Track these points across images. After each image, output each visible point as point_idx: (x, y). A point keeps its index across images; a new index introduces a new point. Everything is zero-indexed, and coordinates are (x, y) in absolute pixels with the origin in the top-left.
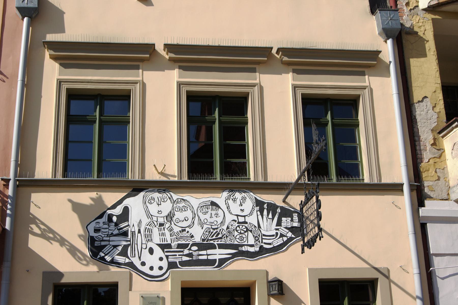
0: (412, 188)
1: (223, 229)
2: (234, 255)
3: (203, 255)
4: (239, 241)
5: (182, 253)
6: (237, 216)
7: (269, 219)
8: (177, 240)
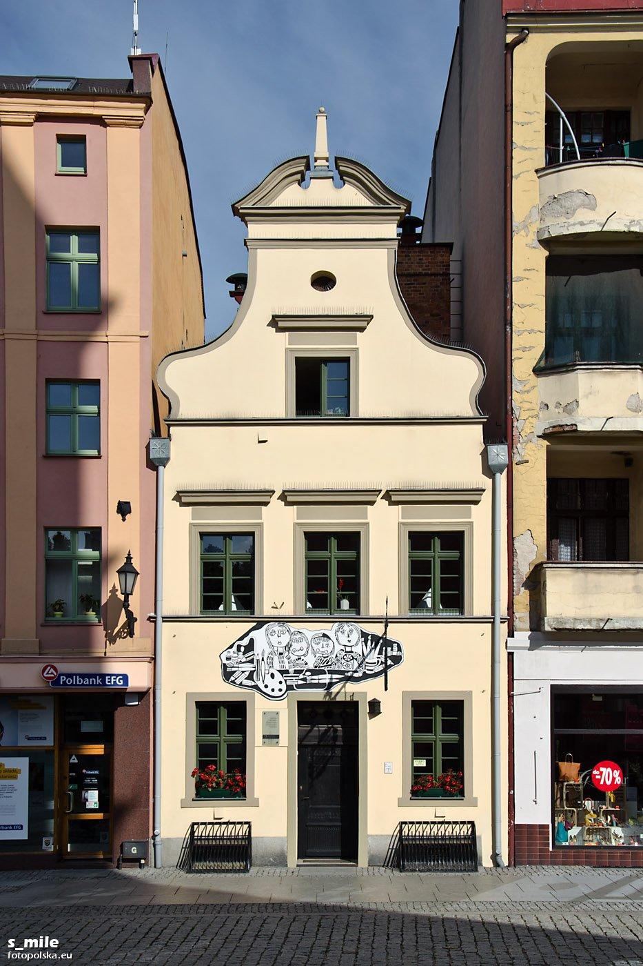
3: (316, 679)
6: (345, 646)
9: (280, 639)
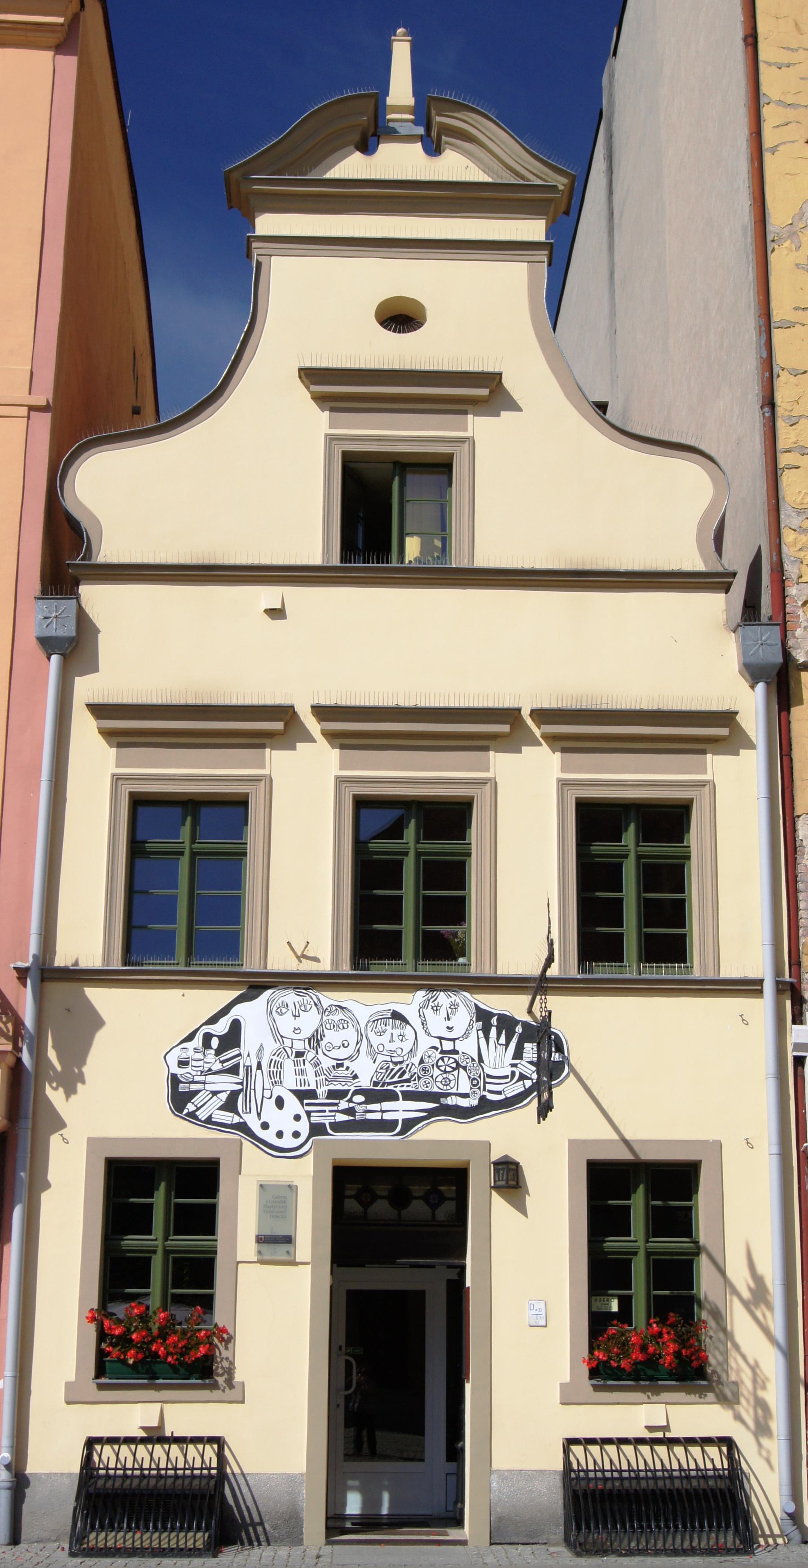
0: (781, 988)
1: (413, 1064)
2: (431, 1113)
3: (376, 1111)
4: (441, 1087)
5: (335, 1108)
7: (500, 1045)
8: (327, 1083)
9: (297, 1023)
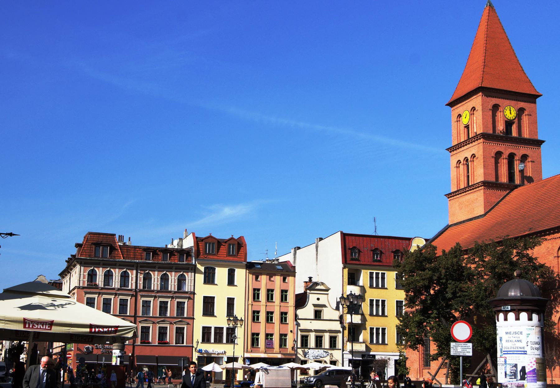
3: (317, 357)
